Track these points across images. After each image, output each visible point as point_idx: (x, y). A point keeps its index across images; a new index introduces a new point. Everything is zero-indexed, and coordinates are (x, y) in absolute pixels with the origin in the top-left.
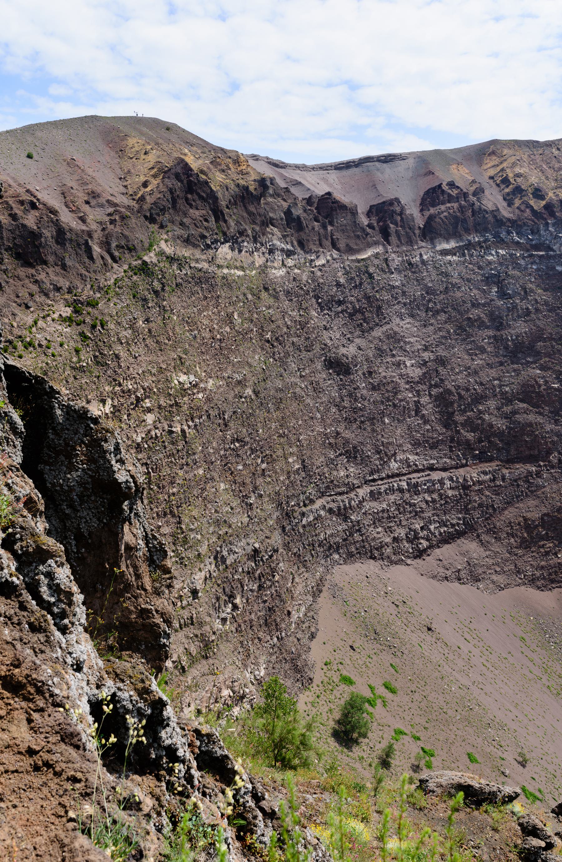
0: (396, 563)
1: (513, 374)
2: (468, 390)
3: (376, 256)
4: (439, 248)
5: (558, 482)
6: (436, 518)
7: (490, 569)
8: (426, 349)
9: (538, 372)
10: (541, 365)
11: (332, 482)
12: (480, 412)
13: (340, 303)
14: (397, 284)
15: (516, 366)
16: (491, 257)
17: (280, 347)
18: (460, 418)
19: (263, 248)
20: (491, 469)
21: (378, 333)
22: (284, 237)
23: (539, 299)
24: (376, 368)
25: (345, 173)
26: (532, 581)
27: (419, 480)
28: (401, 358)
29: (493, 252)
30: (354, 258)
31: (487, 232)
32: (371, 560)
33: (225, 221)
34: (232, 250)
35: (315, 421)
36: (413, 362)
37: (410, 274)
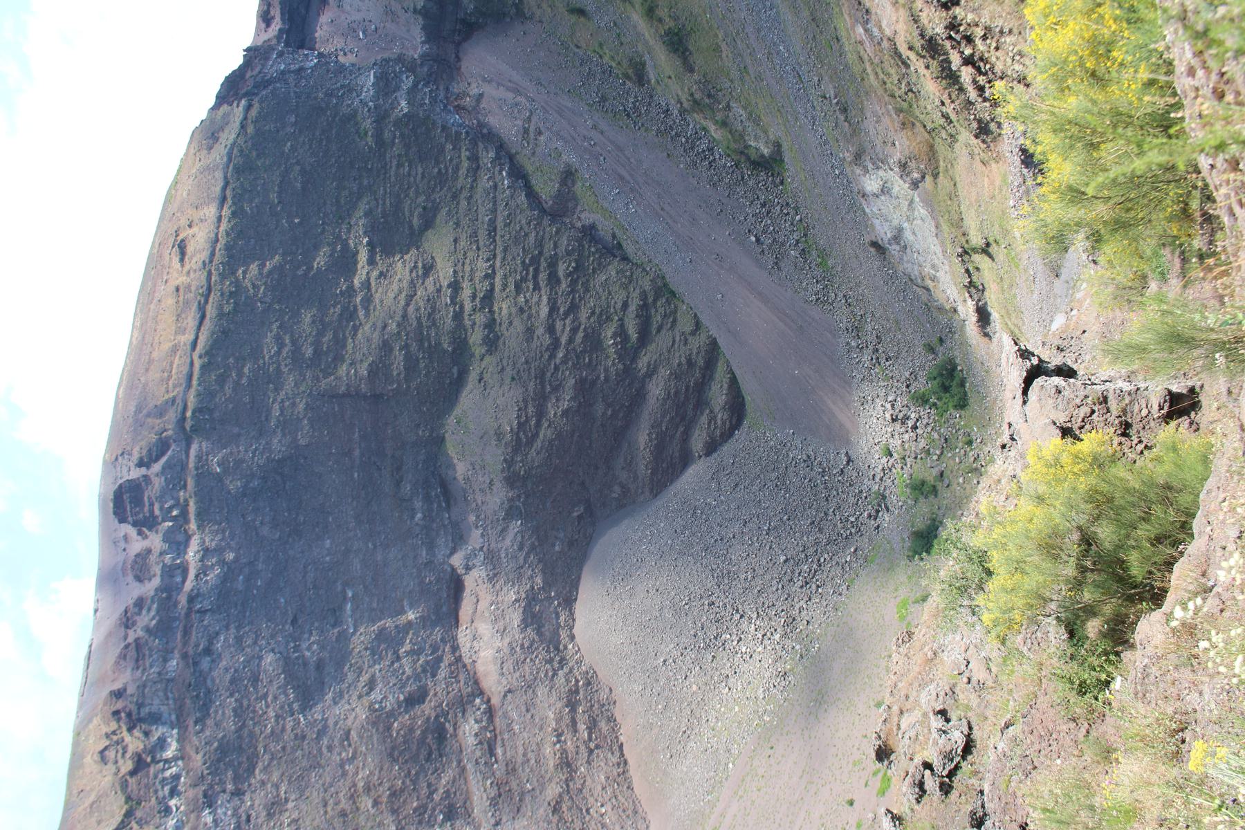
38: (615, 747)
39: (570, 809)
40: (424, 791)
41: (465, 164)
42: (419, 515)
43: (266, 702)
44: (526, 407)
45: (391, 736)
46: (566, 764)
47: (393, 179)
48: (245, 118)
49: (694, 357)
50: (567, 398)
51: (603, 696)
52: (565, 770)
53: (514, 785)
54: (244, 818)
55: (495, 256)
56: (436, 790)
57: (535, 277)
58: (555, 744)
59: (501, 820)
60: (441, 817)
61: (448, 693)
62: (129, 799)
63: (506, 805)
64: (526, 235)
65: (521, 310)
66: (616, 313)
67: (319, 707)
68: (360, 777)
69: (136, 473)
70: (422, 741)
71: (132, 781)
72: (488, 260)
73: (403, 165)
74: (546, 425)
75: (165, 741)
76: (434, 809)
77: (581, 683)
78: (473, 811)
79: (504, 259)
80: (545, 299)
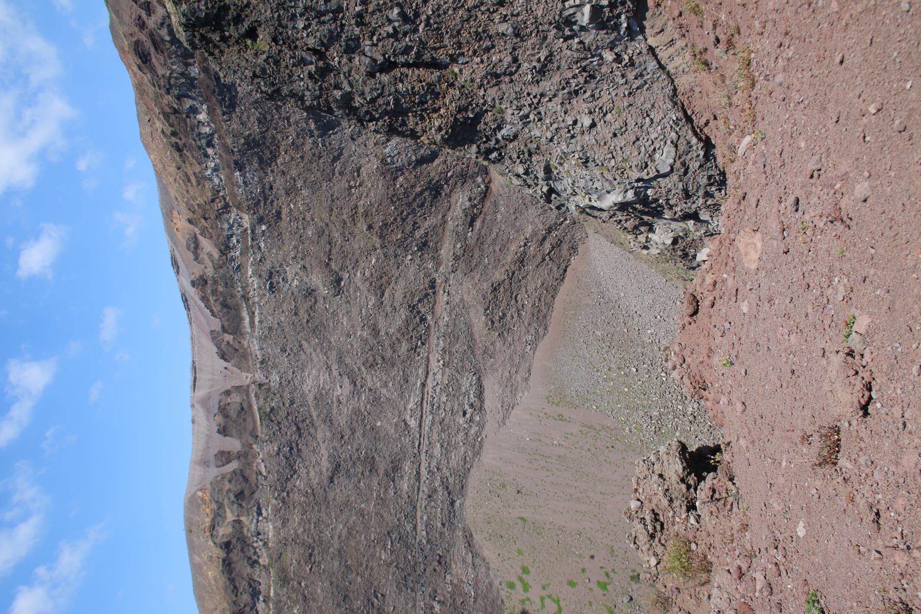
0: (481, 447)
1: (358, 294)
2: (366, 340)
3: (257, 396)
4: (249, 330)
5: (461, 284)
6: (461, 398)
7: (511, 377)
8: (329, 368)
9: (359, 274)
10: (353, 268)
11: (409, 497)
12: (387, 334)
13: (291, 448)
14: (278, 379)
15: (351, 290)
16: (255, 282)
17: (315, 551)
18: (388, 354)
19: (258, 550)
20: (435, 337)
21: (314, 414)
22: (248, 515)
23: (292, 254)
24: (339, 429)
25: (191, 307)
26: (537, 338)
27: (429, 407)
28: (335, 399)
29: (251, 280)
30: (259, 428)
31: (233, 279)
32: (471, 470)
33: (245, 606)
34: (260, 593)
35: (366, 512)
36: (338, 384)
37: (270, 363)
38: (563, 266)
39: (505, 291)
40: (409, 228)
43: (288, 122)
45: (395, 185)
46: (521, 261)
51: (578, 236)
52: (517, 265)
53: (476, 255)
54: (267, 186)
56: (419, 227)
58: (520, 247)
59: (456, 270)
60: (416, 249)
61: (457, 164)
62: (171, 125)
63: (464, 264)
67: (339, 135)
68: (362, 203)
70: (422, 192)
71: (172, 118)
75: (197, 108)
76: (412, 241)
77: (568, 222)
78: (441, 250)
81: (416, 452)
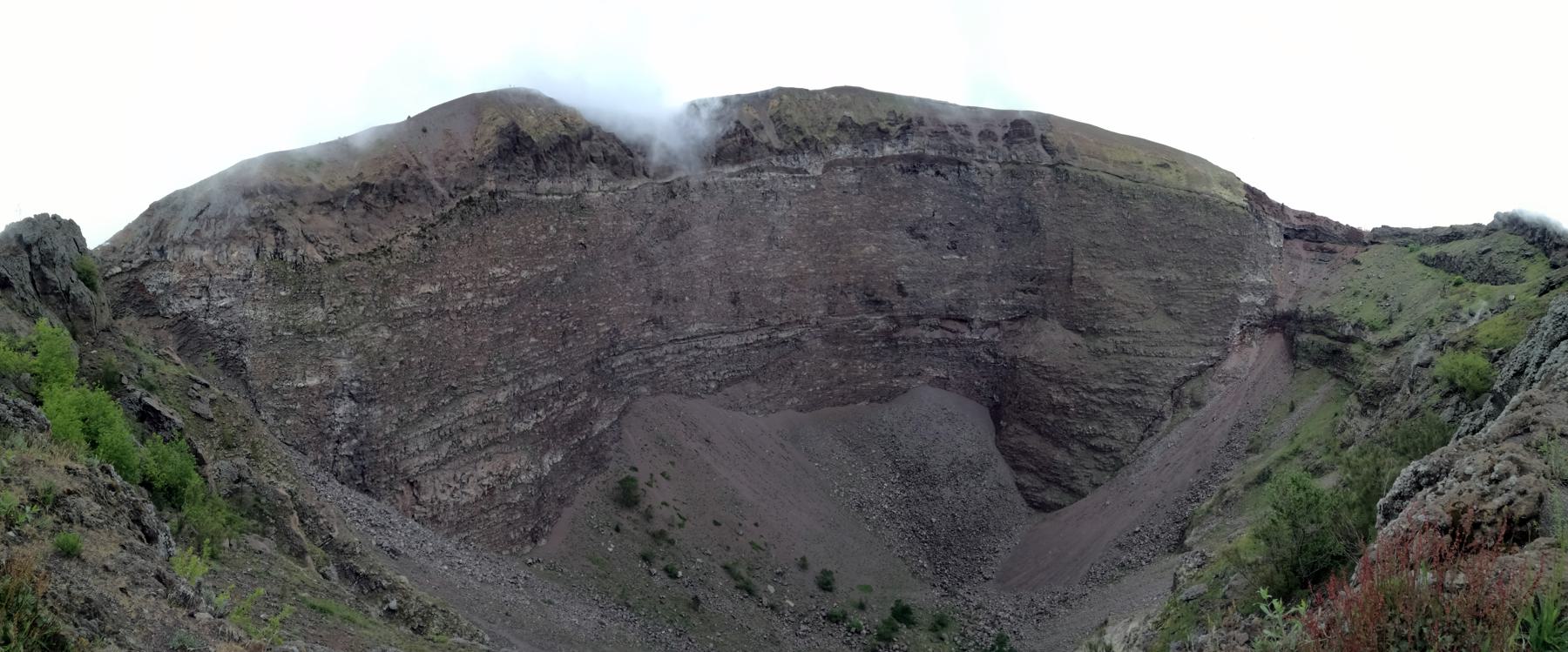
32: (673, 395)
41: (1208, 338)
42: (1004, 302)
44: (1055, 372)
47: (1200, 294)
48: (1236, 205)
49: (1077, 482)
50: (1059, 398)
55: (1148, 356)
57: (1133, 381)
64: (1159, 376)
65: (1113, 372)
66: (1108, 432)
69: (1038, 133)
72: (1145, 352)
73: (1208, 300)
74: (1043, 384)
79: (1145, 362)
80: (1119, 387)
81: (672, 338)
